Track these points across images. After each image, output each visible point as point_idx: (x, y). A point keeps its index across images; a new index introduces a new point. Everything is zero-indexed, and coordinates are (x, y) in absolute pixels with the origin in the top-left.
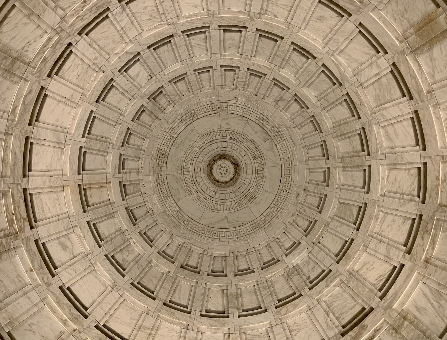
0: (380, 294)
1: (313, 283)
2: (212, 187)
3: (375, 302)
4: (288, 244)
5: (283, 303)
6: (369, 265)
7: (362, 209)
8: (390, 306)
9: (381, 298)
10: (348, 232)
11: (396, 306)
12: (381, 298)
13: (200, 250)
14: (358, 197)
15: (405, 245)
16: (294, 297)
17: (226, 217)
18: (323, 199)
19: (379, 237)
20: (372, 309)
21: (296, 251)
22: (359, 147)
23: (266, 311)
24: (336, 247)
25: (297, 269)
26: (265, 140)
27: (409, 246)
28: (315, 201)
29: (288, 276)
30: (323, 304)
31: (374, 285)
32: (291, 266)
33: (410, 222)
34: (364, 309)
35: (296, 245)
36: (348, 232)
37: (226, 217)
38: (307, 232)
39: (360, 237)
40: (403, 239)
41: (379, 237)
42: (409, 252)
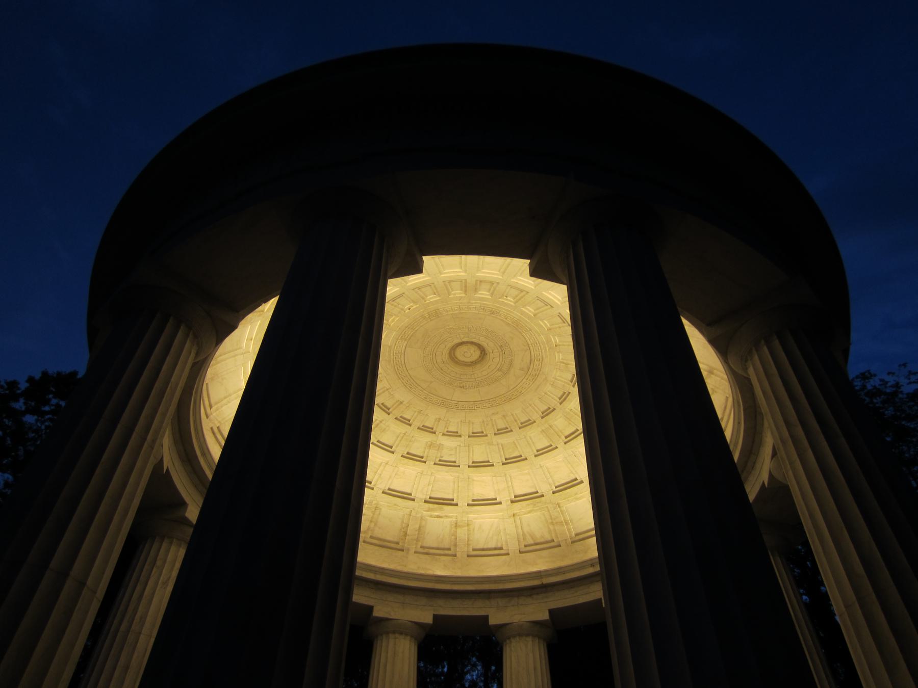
0: (471, 502)
1: (442, 463)
2: (446, 357)
3: (463, 503)
4: (452, 428)
5: (410, 456)
6: (484, 484)
7: (519, 459)
8: (467, 513)
9: (469, 505)
10: (496, 459)
11: (471, 516)
12: (469, 505)
13: (388, 386)
14: (528, 452)
15: (516, 497)
16: (420, 459)
17: (431, 382)
18: (505, 431)
19: (509, 479)
20: (457, 505)
21: (452, 438)
22: (567, 433)
23: (393, 453)
24: (478, 458)
25: (440, 447)
26: (522, 369)
27: (517, 499)
28: (501, 424)
29: (431, 446)
30: (433, 478)
31: (473, 494)
32: (438, 443)
33: (534, 490)
34: (453, 500)
35: (456, 434)
36: (496, 459)
37: (431, 382)
38: (474, 435)
39: (498, 468)
40: (519, 492)
41: (509, 479)
42: (512, 502)
